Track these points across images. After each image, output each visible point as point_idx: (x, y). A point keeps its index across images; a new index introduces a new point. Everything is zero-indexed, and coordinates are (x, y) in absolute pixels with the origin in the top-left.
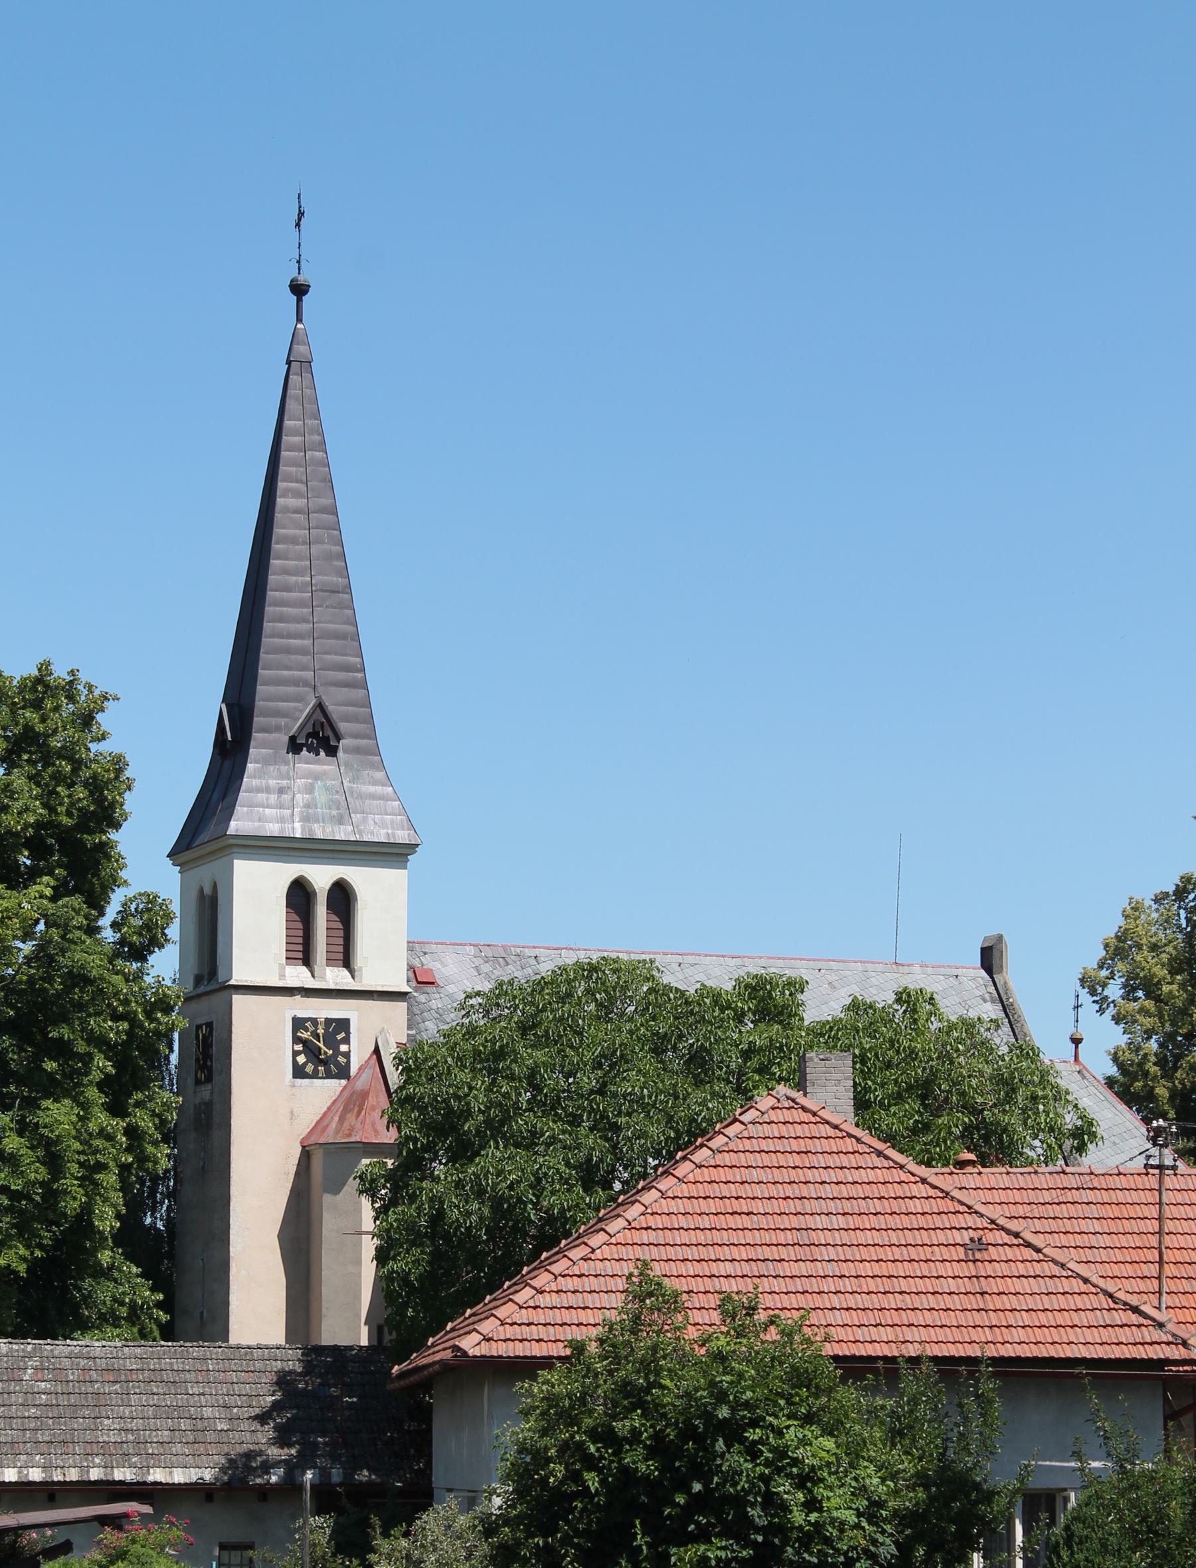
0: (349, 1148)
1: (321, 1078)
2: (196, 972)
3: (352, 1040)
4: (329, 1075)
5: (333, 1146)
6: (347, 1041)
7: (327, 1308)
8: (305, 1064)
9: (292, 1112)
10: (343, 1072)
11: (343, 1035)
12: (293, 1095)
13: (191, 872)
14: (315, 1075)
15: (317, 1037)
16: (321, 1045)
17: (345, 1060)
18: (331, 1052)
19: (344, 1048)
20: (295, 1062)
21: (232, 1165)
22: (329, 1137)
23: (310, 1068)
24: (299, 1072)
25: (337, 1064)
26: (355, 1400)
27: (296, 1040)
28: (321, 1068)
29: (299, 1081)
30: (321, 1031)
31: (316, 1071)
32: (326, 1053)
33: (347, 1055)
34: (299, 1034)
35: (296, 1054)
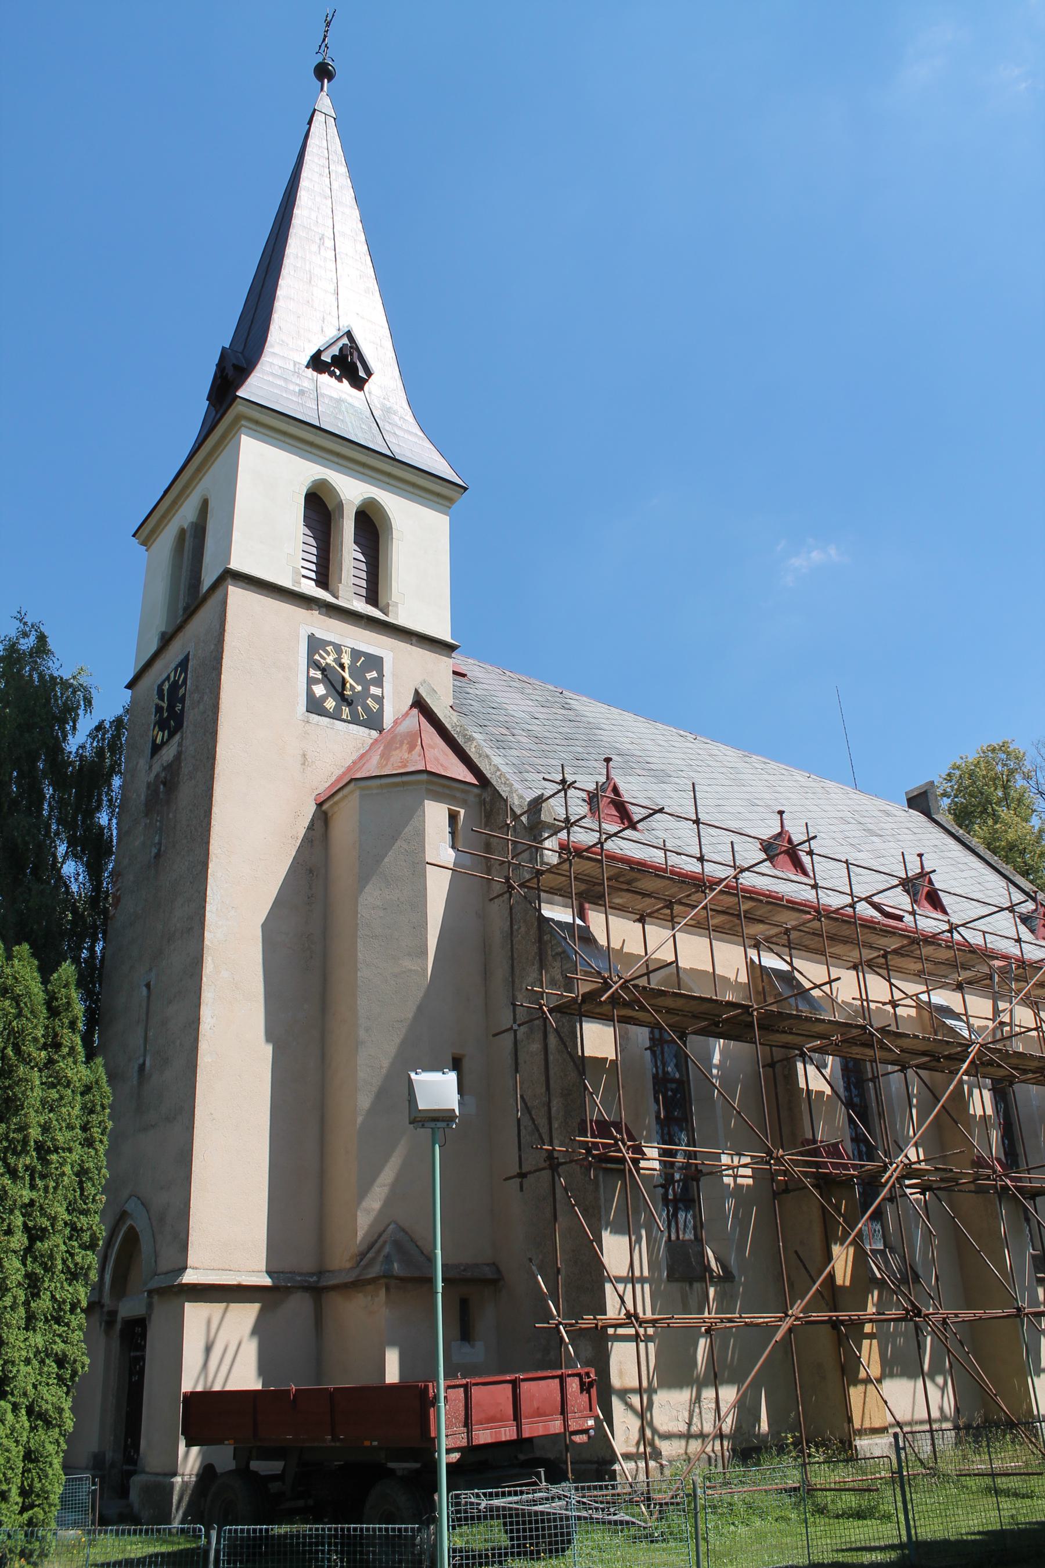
0: (404, 784)
1: (344, 721)
2: (163, 629)
3: (385, 684)
4: (355, 720)
5: (378, 782)
6: (379, 682)
7: (367, 1030)
8: (324, 698)
9: (304, 755)
10: (374, 721)
11: (374, 674)
12: (306, 733)
13: (154, 546)
14: (336, 716)
15: (342, 666)
16: (346, 675)
17: (377, 707)
18: (359, 688)
19: (374, 690)
20: (310, 694)
21: (215, 810)
22: (372, 768)
23: (330, 704)
24: (315, 706)
25: (367, 709)
26: (375, 1443)
27: (313, 664)
28: (346, 711)
29: (315, 718)
30: (346, 660)
31: (338, 709)
32: (352, 688)
33: (379, 700)
34: (317, 657)
35: (311, 681)
